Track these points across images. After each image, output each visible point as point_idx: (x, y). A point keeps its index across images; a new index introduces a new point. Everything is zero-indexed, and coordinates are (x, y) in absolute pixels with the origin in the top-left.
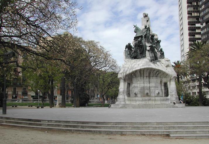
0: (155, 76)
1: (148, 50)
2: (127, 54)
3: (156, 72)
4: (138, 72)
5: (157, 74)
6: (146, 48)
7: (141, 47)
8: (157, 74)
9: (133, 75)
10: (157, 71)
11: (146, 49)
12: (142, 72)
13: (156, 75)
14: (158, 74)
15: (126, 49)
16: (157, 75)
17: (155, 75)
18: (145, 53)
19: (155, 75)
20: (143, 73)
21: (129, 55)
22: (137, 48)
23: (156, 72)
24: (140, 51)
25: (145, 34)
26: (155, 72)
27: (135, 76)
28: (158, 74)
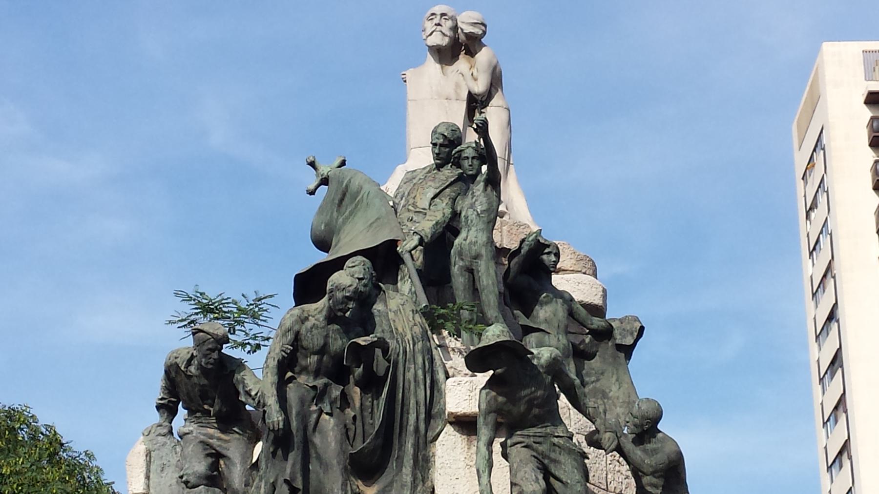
1: (466, 425)
2: (171, 476)
6: (434, 390)
7: (371, 384)
11: (432, 409)
15: (168, 409)
18: (423, 464)
22: (320, 395)
24: (346, 435)
25: (427, 226)
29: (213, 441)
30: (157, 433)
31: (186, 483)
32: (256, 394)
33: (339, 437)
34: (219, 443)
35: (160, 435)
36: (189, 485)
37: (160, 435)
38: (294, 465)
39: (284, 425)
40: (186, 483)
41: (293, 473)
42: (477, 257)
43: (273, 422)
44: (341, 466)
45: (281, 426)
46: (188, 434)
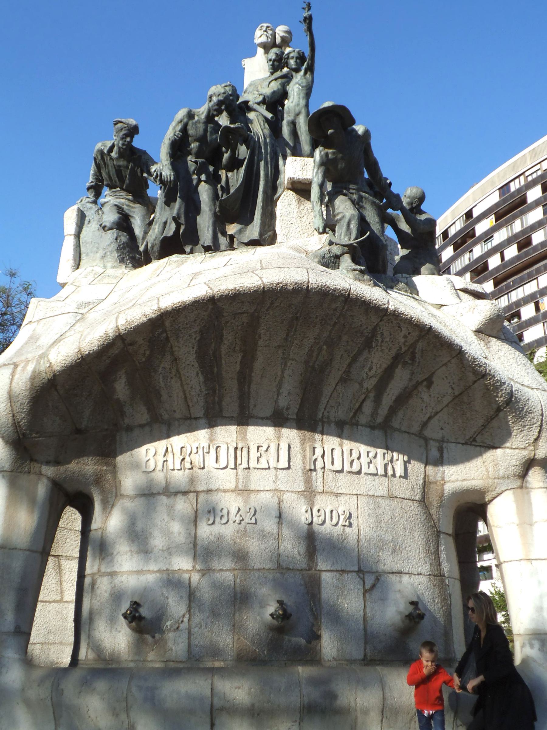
0: (363, 419)
3: (387, 376)
4: (186, 351)
5: (388, 399)
8: (388, 399)
9: (121, 388)
10: (397, 359)
12: (230, 366)
13: (383, 411)
14: (402, 399)
16: (393, 411)
17: (368, 408)
19: (368, 408)
20: (244, 378)
21: (111, 235)
23: (387, 376)
26: (378, 360)
27: (141, 415)
28: (402, 399)
29: (125, 207)
30: (86, 201)
31: (104, 228)
32: (155, 171)
33: (211, 196)
34: (127, 208)
35: (88, 202)
36: (106, 229)
37: (88, 202)
38: (179, 209)
39: (174, 178)
40: (104, 228)
41: (178, 214)
42: (298, 114)
43: (167, 176)
44: (212, 212)
45: (172, 179)
46: (107, 202)
